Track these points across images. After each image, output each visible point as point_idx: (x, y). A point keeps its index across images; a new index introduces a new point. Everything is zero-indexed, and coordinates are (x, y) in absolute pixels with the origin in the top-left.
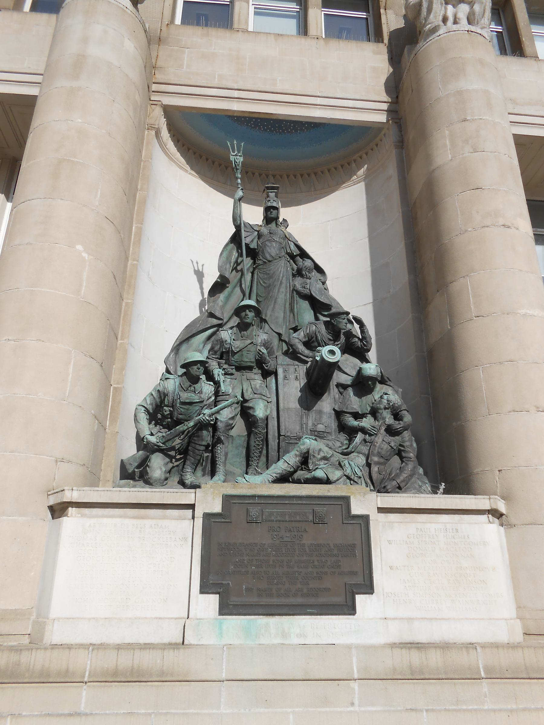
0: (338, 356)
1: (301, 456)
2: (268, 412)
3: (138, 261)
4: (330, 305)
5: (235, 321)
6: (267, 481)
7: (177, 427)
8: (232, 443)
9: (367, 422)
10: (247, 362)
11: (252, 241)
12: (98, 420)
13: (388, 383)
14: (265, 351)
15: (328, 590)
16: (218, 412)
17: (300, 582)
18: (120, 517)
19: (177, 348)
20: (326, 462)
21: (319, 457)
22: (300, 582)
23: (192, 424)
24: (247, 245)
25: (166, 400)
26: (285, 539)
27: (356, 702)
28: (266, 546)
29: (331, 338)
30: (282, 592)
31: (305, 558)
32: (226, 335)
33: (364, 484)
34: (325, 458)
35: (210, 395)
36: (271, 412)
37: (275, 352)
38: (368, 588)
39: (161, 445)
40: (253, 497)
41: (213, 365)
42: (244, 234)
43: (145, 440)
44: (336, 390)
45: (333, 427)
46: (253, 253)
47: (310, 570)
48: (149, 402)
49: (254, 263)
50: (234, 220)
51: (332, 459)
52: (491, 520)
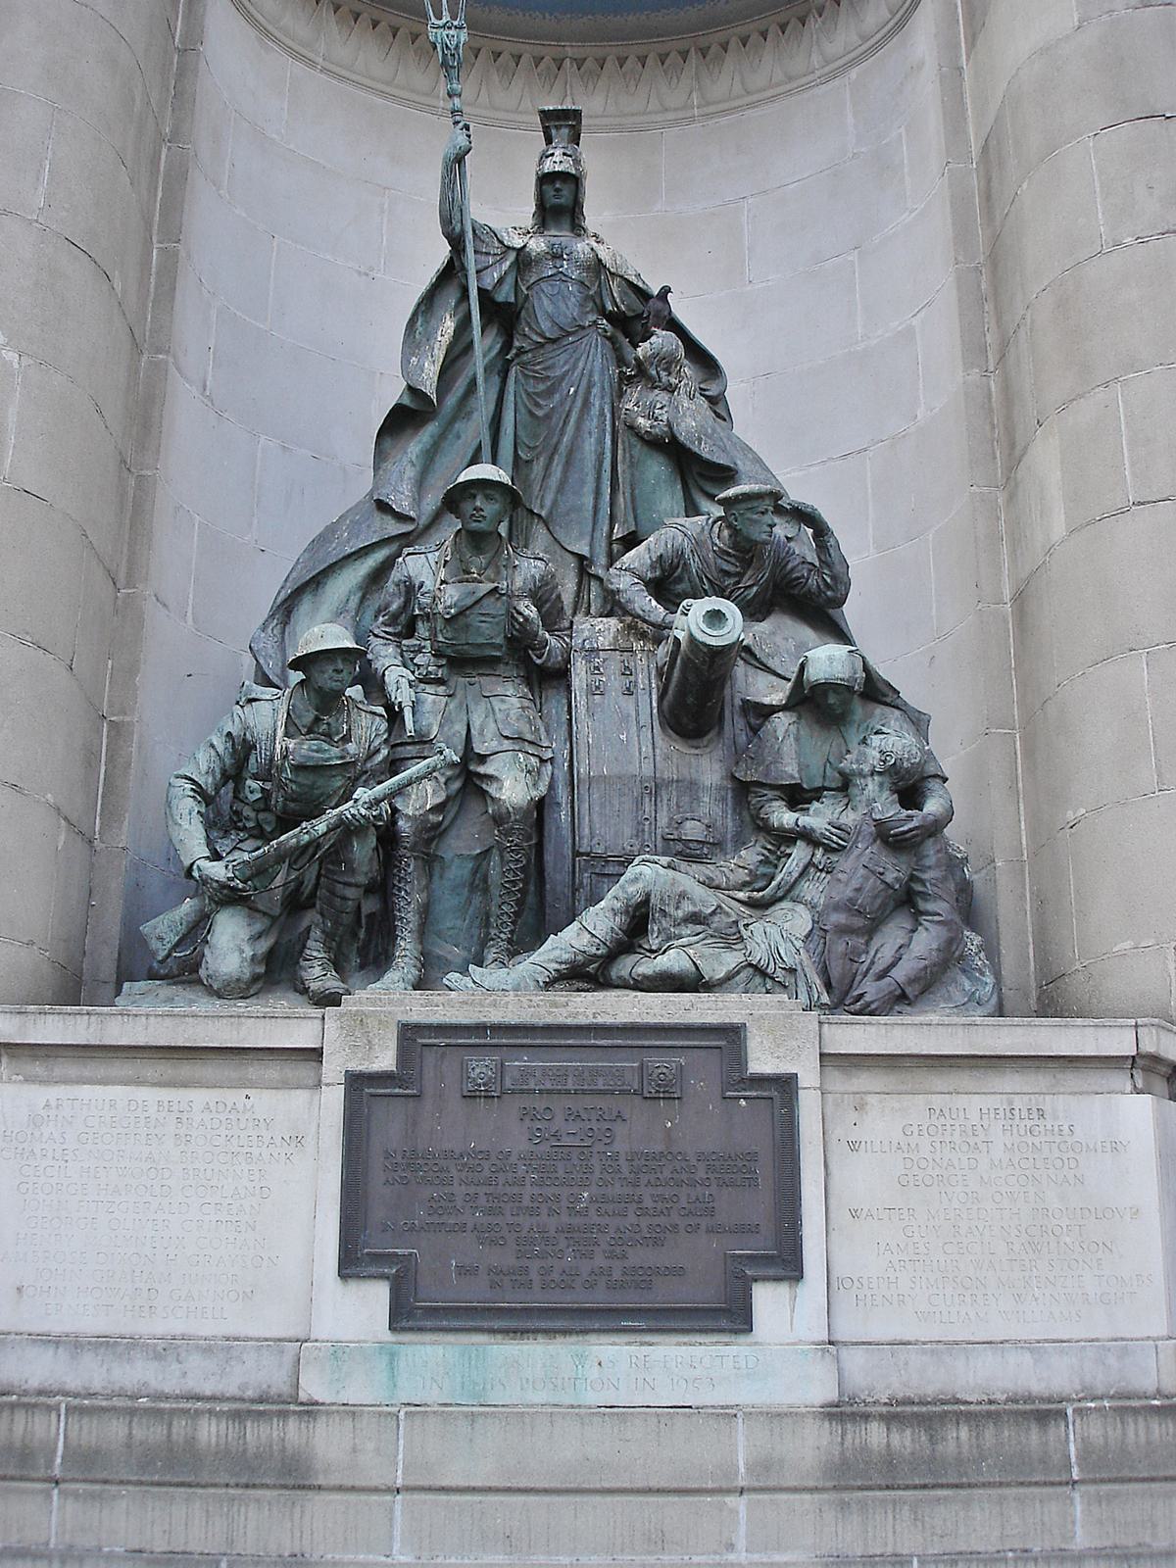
0: (735, 627)
1: (627, 912)
2: (543, 789)
3: (168, 352)
4: (728, 469)
6: (532, 984)
7: (282, 838)
8: (441, 877)
9: (818, 818)
11: (501, 281)
12: (66, 819)
13: (888, 700)
14: (531, 612)
15: (678, 1272)
16: (400, 791)
17: (604, 1252)
18: (126, 1082)
19: (286, 609)
20: (700, 928)
21: (680, 913)
22: (604, 1252)
23: (321, 826)
25: (252, 760)
26: (567, 1141)
27: (741, 1543)
28: (513, 1159)
30: (555, 1276)
31: (617, 1190)
32: (421, 566)
33: (802, 989)
34: (695, 918)
35: (376, 743)
36: (551, 787)
37: (569, 611)
38: (788, 1265)
39: (241, 886)
40: (480, 1029)
41: (385, 657)
42: (471, 260)
43: (196, 874)
44: (740, 723)
45: (730, 824)
46: (503, 315)
47: (632, 1219)
48: (204, 768)
49: (507, 346)
50: (446, 221)
51: (716, 918)
52: (1140, 1085)
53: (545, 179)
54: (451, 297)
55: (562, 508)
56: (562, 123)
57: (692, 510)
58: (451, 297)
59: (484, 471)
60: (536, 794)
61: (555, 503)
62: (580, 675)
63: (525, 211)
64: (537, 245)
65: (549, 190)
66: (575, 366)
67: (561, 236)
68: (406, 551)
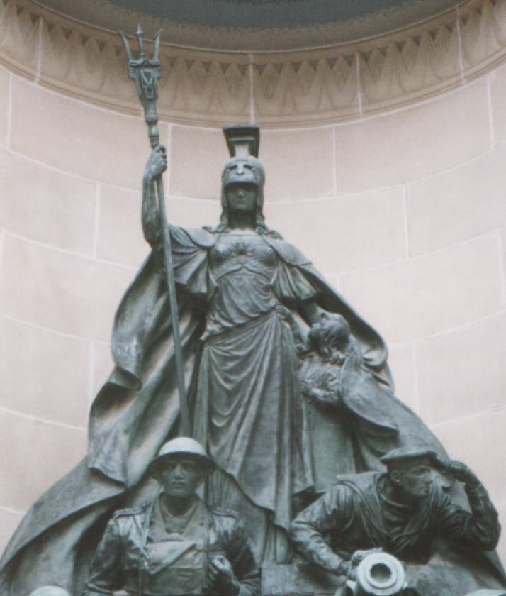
5: (153, 490)
14: (226, 566)
24: (179, 287)
29: (395, 519)
37: (257, 560)
53: (230, 188)
54: (152, 287)
55: (251, 468)
56: (243, 137)
57: (362, 466)
58: (152, 287)
59: (183, 444)
63: (212, 212)
64: (223, 245)
65: (231, 195)
66: (258, 346)
67: (246, 236)
68: (118, 513)
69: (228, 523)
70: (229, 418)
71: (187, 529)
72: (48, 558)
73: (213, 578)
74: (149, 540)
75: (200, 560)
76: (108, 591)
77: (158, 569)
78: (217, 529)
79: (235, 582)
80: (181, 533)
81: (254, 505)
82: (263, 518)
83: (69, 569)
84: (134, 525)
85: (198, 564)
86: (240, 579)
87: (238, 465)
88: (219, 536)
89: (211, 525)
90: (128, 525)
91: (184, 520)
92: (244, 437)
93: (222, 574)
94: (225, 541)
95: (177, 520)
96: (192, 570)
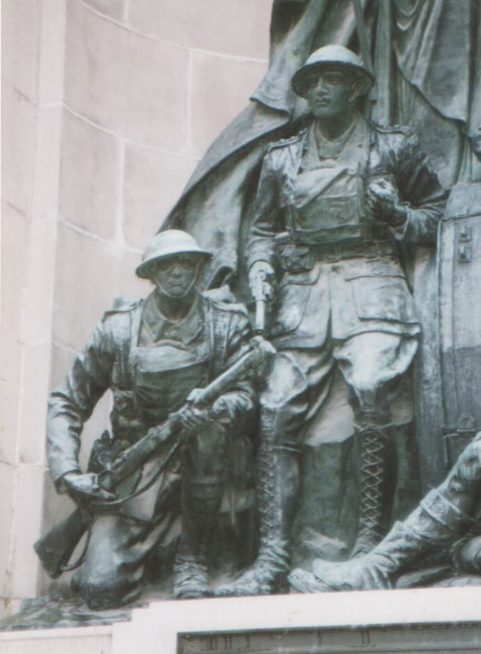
2: (402, 365)
10: (332, 231)
39: (106, 495)
55: (439, 74)
60: (389, 374)
61: (430, 72)
62: (448, 240)
69: (394, 142)
70: (414, 18)
71: (341, 155)
72: (213, 205)
73: (372, 205)
74: (301, 171)
75: (354, 186)
76: (271, 233)
77: (304, 202)
78: (380, 149)
79: (398, 208)
80: (335, 159)
81: (445, 118)
82: (455, 132)
83: (236, 211)
84: (289, 157)
85: (350, 192)
86: (416, 205)
87: (423, 74)
88: (383, 157)
89: (373, 146)
90: (282, 159)
91: (338, 144)
92: (429, 38)
93: (381, 199)
94: (393, 164)
95: (332, 145)
96: (347, 199)
